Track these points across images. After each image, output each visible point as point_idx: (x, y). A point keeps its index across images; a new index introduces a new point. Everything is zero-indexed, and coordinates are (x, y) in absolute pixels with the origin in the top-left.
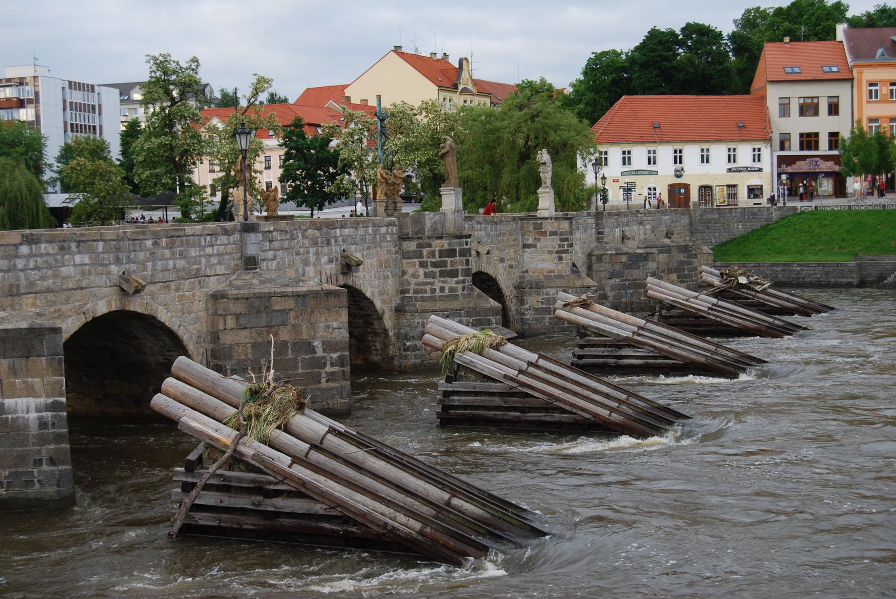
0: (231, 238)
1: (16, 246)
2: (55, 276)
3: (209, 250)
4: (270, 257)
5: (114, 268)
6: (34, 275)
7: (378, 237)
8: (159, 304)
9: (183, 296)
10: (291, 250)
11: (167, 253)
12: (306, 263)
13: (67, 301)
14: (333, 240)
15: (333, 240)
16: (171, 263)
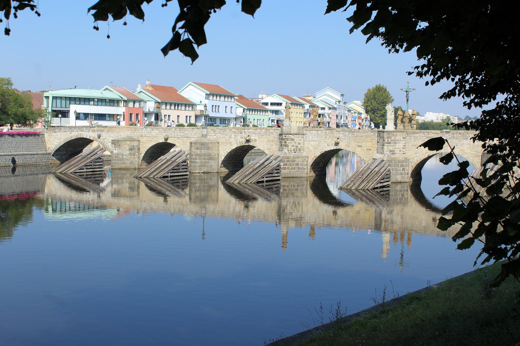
0: (199, 130)
1: (143, 128)
2: (150, 134)
3: (192, 132)
4: (213, 135)
5: (164, 134)
6: (146, 134)
7: (268, 133)
8: (177, 142)
9: (183, 141)
10: (224, 134)
11: (179, 132)
12: (230, 137)
13: (153, 139)
14: (243, 133)
15: (243, 133)
16: (179, 134)
